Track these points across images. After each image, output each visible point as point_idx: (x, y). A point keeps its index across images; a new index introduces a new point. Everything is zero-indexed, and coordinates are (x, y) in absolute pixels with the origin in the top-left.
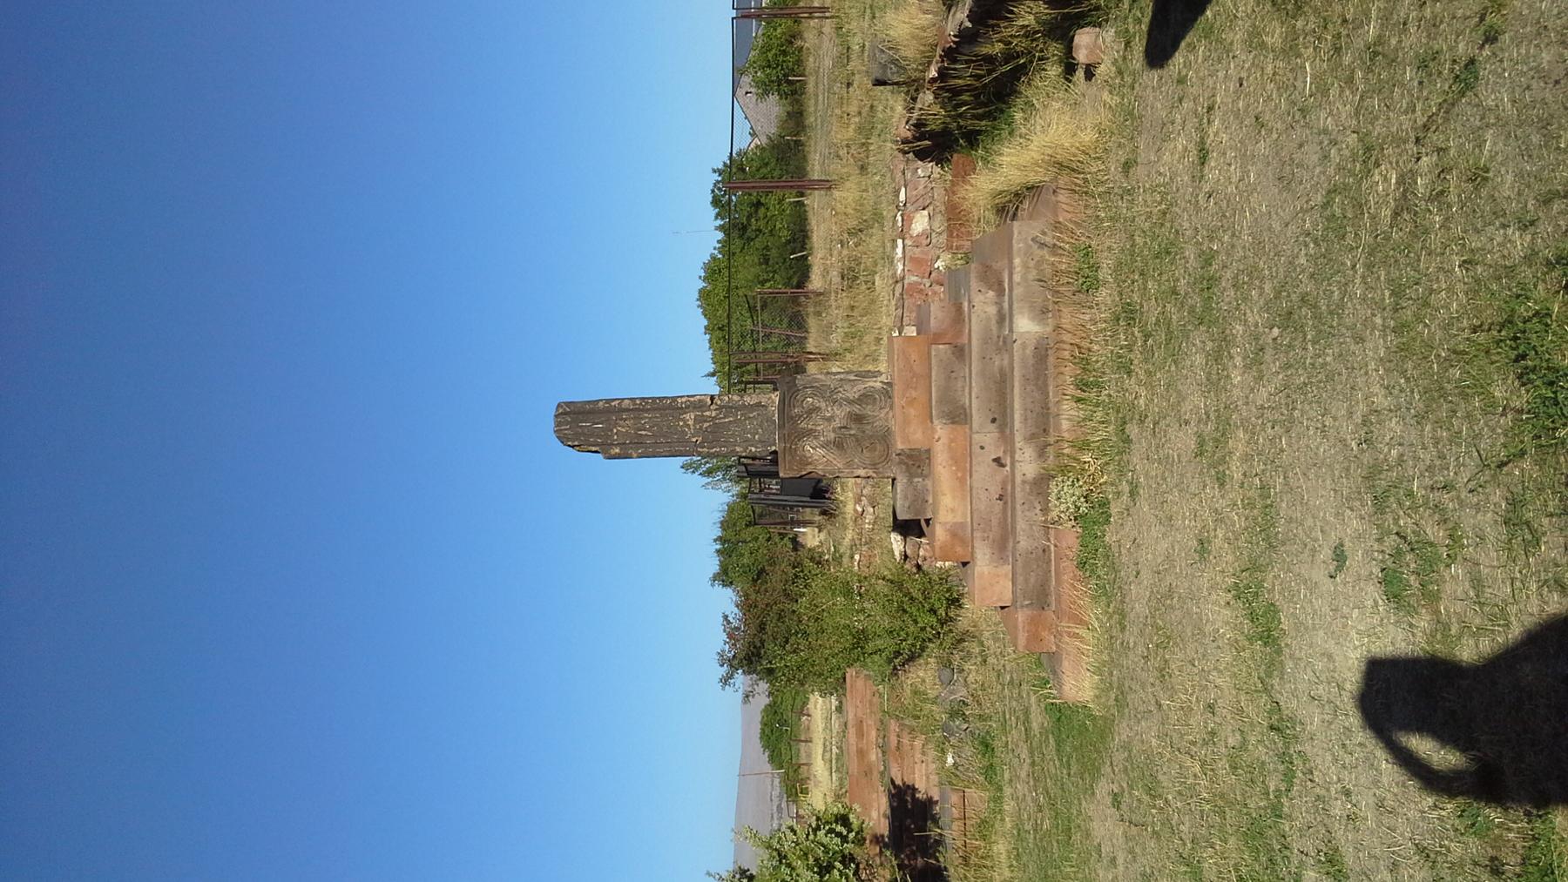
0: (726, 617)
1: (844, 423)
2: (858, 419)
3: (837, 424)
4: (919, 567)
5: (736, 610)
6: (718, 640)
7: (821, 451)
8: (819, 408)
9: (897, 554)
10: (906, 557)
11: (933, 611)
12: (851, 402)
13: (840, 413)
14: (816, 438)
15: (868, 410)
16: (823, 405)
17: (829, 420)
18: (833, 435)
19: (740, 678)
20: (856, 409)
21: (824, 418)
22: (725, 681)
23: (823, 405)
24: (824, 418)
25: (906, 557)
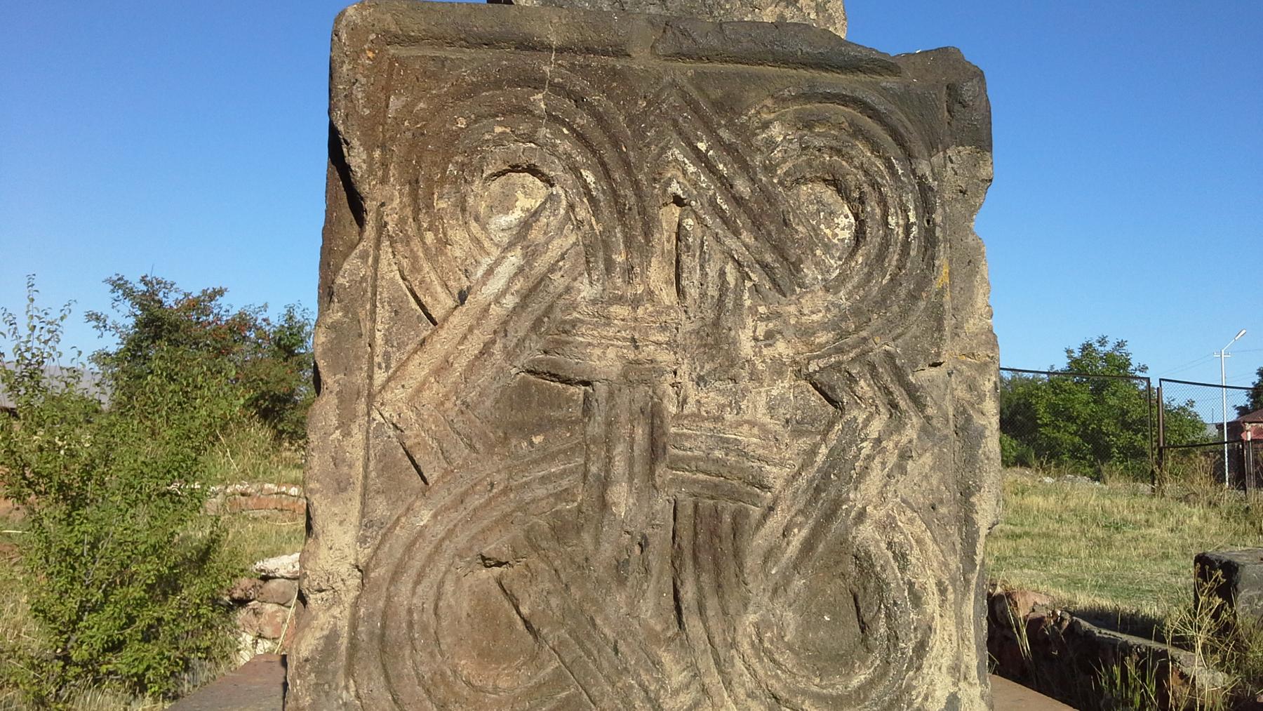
0: (220, 292)
1: (692, 441)
2: (708, 541)
3: (688, 395)
4: (242, 602)
5: (234, 312)
6: (184, 281)
7: (499, 282)
8: (783, 267)
9: (270, 564)
10: (266, 579)
11: (115, 647)
12: (826, 495)
13: (753, 418)
14: (594, 251)
15: (768, 616)
16: (813, 307)
17: (713, 342)
18: (603, 357)
19: (124, 316)
20: (779, 530)
21: (722, 306)
22: (119, 284)
23: (813, 307)
24: (722, 306)
25: (266, 579)
